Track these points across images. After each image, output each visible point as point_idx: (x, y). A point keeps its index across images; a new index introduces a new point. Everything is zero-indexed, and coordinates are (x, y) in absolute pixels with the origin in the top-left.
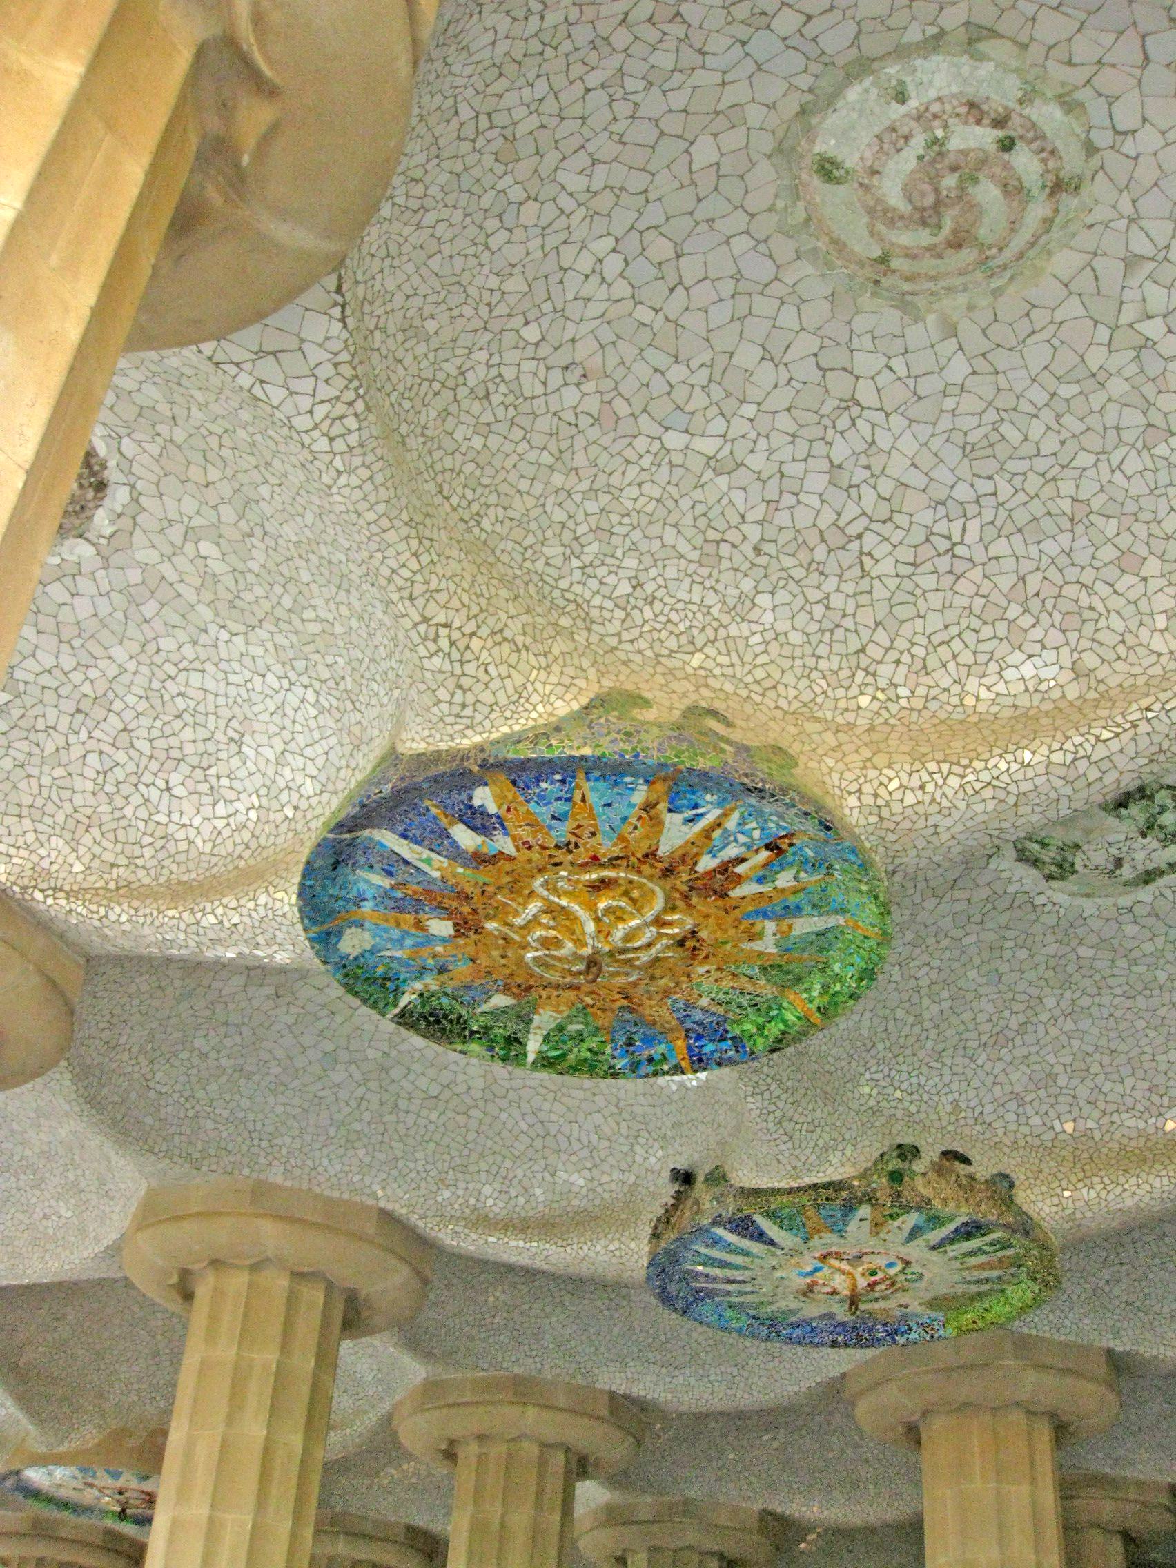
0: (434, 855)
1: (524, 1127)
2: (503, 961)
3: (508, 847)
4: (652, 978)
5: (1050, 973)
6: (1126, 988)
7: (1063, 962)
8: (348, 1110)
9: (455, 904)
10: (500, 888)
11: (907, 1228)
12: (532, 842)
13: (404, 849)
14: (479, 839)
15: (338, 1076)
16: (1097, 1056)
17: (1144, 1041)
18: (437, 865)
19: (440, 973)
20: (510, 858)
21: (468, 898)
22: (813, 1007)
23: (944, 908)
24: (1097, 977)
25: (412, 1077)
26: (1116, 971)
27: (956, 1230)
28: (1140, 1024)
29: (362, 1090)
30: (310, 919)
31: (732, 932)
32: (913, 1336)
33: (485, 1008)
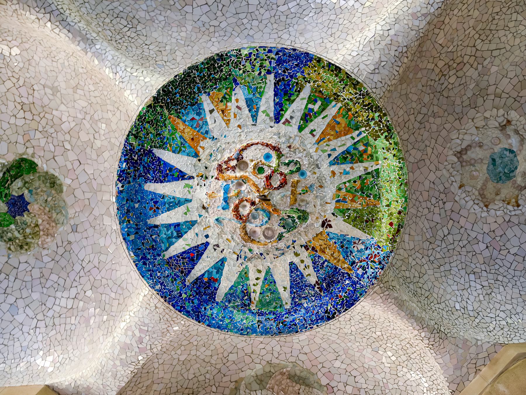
1: (113, 295)
5: (275, 26)
6: (313, 11)
7: (277, 17)
8: (30, 337)
15: (20, 317)
16: (325, 41)
17: (342, 20)
23: (198, 11)
24: (298, 15)
25: (57, 302)
26: (304, 8)
27: (275, 95)
28: (333, 17)
29: (35, 321)
32: (370, 271)
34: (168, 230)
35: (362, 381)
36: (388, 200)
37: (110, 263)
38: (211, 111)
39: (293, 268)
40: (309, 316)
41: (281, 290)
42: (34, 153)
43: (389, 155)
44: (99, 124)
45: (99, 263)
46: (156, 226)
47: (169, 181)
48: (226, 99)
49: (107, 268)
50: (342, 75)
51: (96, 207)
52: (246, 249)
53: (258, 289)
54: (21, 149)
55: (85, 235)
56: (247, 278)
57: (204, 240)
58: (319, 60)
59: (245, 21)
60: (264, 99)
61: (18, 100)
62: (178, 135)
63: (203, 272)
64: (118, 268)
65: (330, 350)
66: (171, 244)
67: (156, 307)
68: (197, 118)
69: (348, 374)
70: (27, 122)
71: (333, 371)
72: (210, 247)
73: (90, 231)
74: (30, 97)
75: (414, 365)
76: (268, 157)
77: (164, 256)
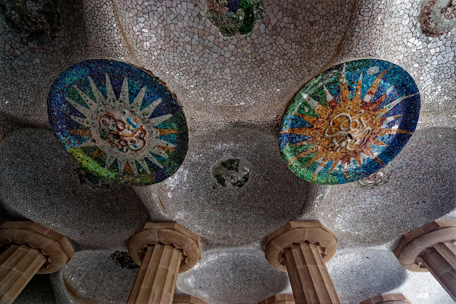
0: (390, 109)
2: (347, 107)
3: (383, 127)
4: (322, 137)
9: (374, 107)
10: (372, 119)
11: (161, 155)
12: (381, 132)
13: (394, 103)
14: (388, 122)
18: (387, 109)
19: (348, 87)
20: (379, 126)
21: (374, 111)
22: (292, 163)
30: (396, 69)
31: (329, 157)
33: (325, 89)
34: (136, 90)
35: (20, 63)
36: (90, 162)
37: (165, 18)
38: (167, 145)
39: (83, 116)
40: (55, 104)
41: (77, 104)
42: (246, 39)
43: (105, 175)
44: (222, 84)
45: (171, 11)
46: (142, 87)
47: (155, 110)
48: (168, 152)
49: (165, 14)
50: (143, 184)
51: (198, 40)
52: (104, 109)
53: (83, 96)
54: (254, 36)
55: (192, 19)
56: (91, 98)
57: (120, 99)
58: (153, 183)
59: (207, 156)
60: (156, 160)
61: (267, 63)
62: (170, 128)
63: (107, 85)
64: (159, 20)
65: (48, 65)
66: (129, 85)
67: (105, 46)
68: (170, 139)
69: (28, 60)
70: (257, 54)
71: (34, 55)
72: (115, 98)
73: (191, 24)
74: (261, 69)
75: (14, 97)
76: (135, 147)
77: (126, 77)
